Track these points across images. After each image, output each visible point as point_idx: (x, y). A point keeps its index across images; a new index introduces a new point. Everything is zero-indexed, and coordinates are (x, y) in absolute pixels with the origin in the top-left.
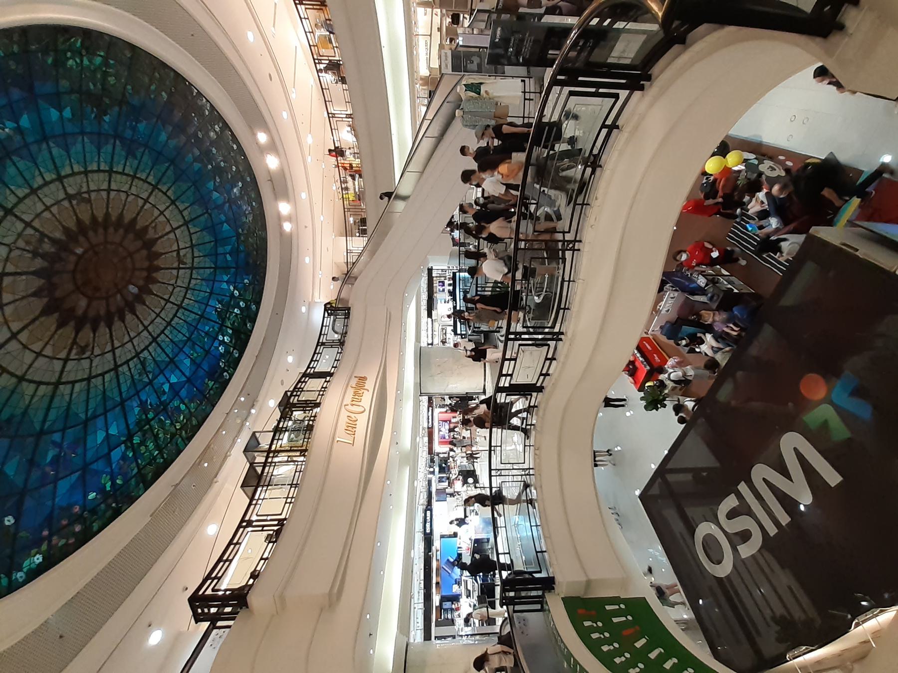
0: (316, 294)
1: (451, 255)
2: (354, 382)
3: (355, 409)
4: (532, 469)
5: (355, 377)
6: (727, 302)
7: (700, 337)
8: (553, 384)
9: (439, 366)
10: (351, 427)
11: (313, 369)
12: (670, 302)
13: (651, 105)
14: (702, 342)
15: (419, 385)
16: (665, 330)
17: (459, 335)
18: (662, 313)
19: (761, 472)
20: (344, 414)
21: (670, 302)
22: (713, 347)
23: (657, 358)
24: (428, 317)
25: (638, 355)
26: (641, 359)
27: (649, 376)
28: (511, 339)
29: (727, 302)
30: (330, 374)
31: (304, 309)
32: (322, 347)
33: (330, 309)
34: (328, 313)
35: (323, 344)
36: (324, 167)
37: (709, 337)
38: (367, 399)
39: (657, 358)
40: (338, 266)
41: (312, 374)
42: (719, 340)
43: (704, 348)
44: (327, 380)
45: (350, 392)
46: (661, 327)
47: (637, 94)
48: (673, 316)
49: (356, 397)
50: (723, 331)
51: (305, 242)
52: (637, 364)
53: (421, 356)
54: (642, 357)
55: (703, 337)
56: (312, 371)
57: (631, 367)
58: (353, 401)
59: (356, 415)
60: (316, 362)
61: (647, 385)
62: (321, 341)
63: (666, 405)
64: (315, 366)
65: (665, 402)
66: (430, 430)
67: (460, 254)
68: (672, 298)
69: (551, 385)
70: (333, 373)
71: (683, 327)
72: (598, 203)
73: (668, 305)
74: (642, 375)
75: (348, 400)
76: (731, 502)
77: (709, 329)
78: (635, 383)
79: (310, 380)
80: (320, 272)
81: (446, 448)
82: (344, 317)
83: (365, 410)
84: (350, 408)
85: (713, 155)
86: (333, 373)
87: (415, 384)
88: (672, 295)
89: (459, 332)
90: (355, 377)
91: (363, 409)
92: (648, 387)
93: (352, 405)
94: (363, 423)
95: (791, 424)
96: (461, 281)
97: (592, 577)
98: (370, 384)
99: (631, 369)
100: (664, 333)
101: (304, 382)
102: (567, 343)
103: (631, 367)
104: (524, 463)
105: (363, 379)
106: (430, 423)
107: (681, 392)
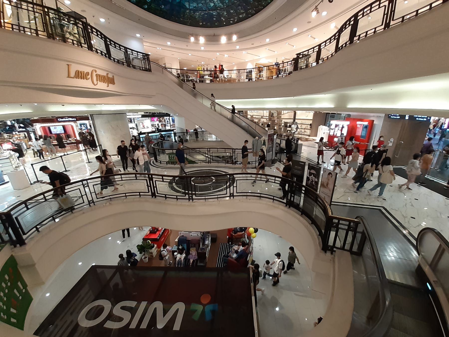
0: (147, 44)
1: (182, 129)
2: (110, 76)
3: (95, 78)
4: (94, 204)
5: (113, 76)
6: (201, 256)
7: (183, 252)
8: (160, 202)
9: (117, 126)
10: (80, 75)
11: (109, 43)
12: (195, 235)
13: (282, 210)
14: (181, 254)
15: (100, 114)
16: (183, 238)
17: (139, 137)
18: (190, 234)
19: (158, 305)
20: (89, 70)
21: (196, 235)
22: (181, 259)
23: (163, 239)
24: (142, 115)
25: (162, 231)
26: (161, 233)
27: (154, 240)
28: (350, 224)
29: (201, 256)
30: (110, 57)
31: (138, 35)
32: (124, 51)
33: (146, 57)
34: (145, 56)
35: (127, 51)
36: (213, 59)
37: (184, 255)
38: (102, 86)
39: (163, 239)
40: (162, 59)
41: (127, 53)
42: (185, 260)
43: (179, 256)
44: (125, 64)
45: (104, 73)
46: (183, 236)
47: (285, 205)
48: (189, 239)
49: (102, 78)
50: (190, 259)
51: (181, 44)
52: (157, 233)
53: (121, 114)
54: (162, 233)
55: (184, 253)
56: (108, 43)
57: (156, 230)
58: (99, 76)
59: (90, 78)
60: (119, 48)
61: (149, 241)
62: (128, 50)
63: (142, 253)
64: (112, 45)
65: (143, 253)
66: (55, 120)
67: (183, 133)
68: (198, 235)
69: (160, 201)
70: (111, 59)
71: (186, 244)
72: (248, 200)
73: (194, 234)
74: (153, 237)
75: (100, 72)
76: (133, 304)
77: (188, 253)
78: (147, 236)
79: (103, 42)
80: (160, 49)
81: (40, 132)
82: (143, 67)
83: (95, 85)
84: (94, 74)
85: (254, 228)
86: (111, 59)
87: (101, 111)
88: (199, 234)
89: (141, 136)
90: (113, 76)
91: (96, 84)
92: (148, 241)
93: (96, 75)
94: (86, 84)
95: (187, 303)
96: (169, 134)
97: (36, 266)
98: (111, 88)
99: (154, 231)
100: (180, 238)
101: (98, 34)
102: (189, 204)
103: (156, 230)
104: (97, 199)
105: (111, 81)
106: (61, 120)
107: (150, 257)
